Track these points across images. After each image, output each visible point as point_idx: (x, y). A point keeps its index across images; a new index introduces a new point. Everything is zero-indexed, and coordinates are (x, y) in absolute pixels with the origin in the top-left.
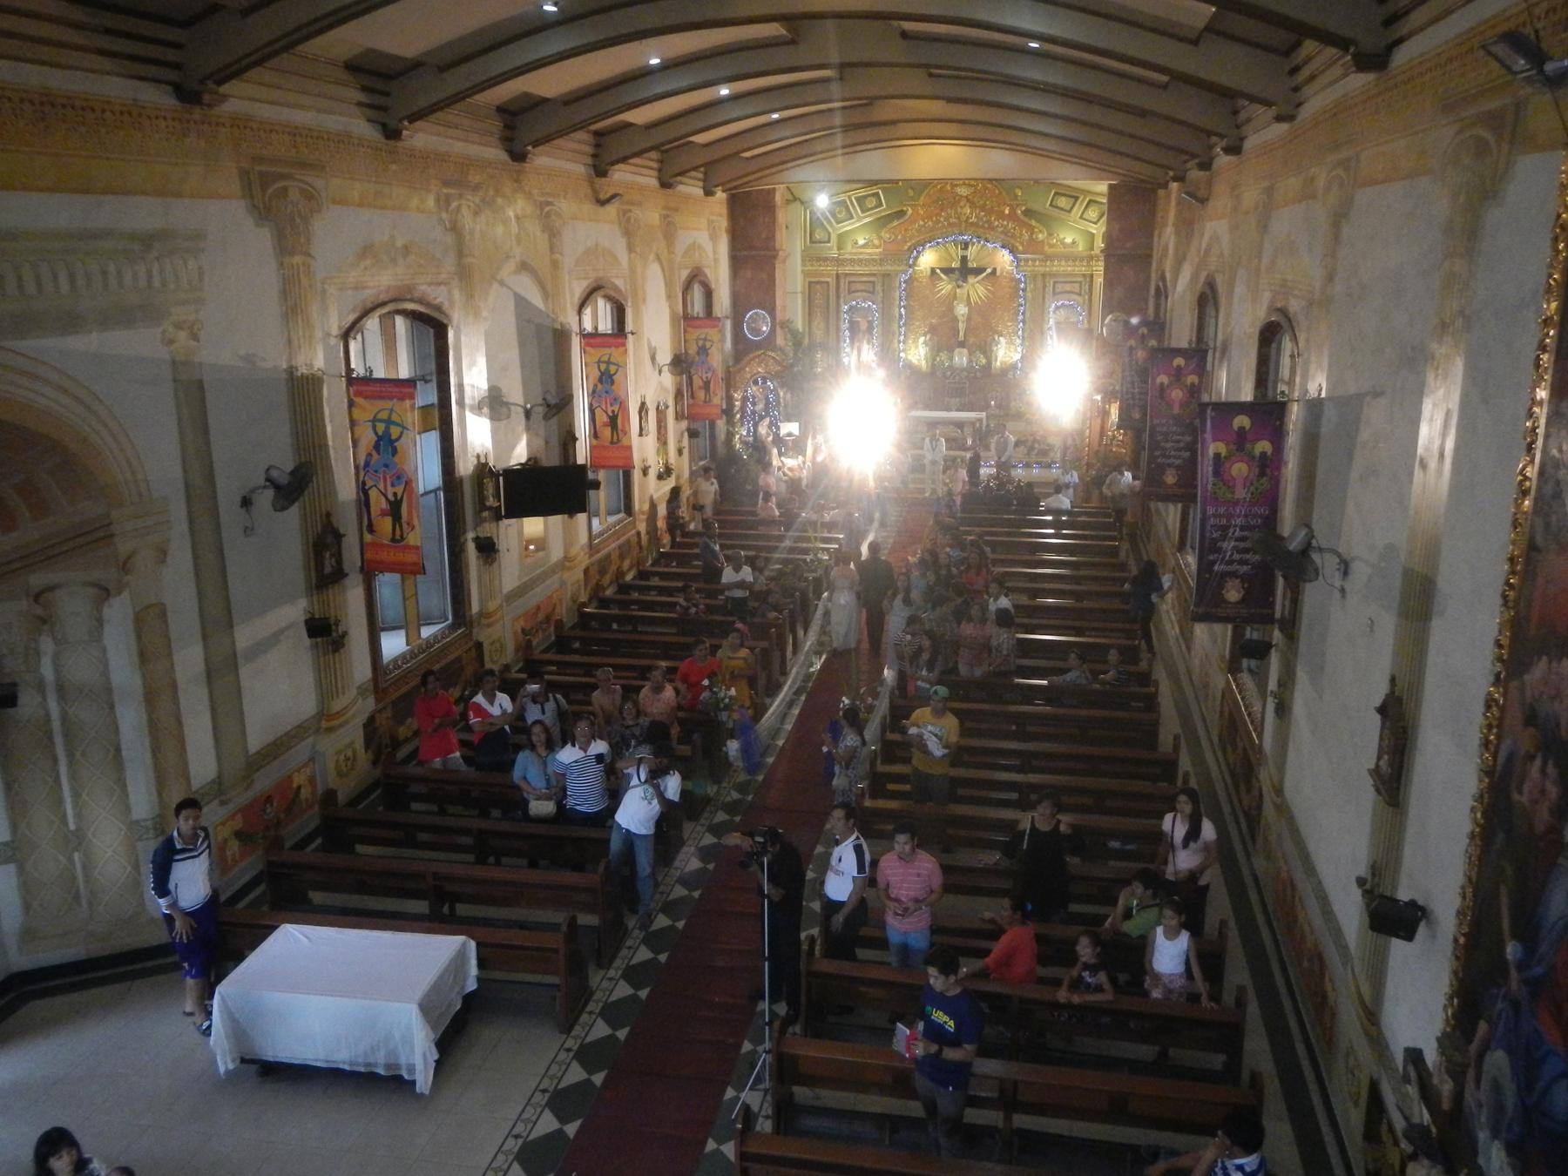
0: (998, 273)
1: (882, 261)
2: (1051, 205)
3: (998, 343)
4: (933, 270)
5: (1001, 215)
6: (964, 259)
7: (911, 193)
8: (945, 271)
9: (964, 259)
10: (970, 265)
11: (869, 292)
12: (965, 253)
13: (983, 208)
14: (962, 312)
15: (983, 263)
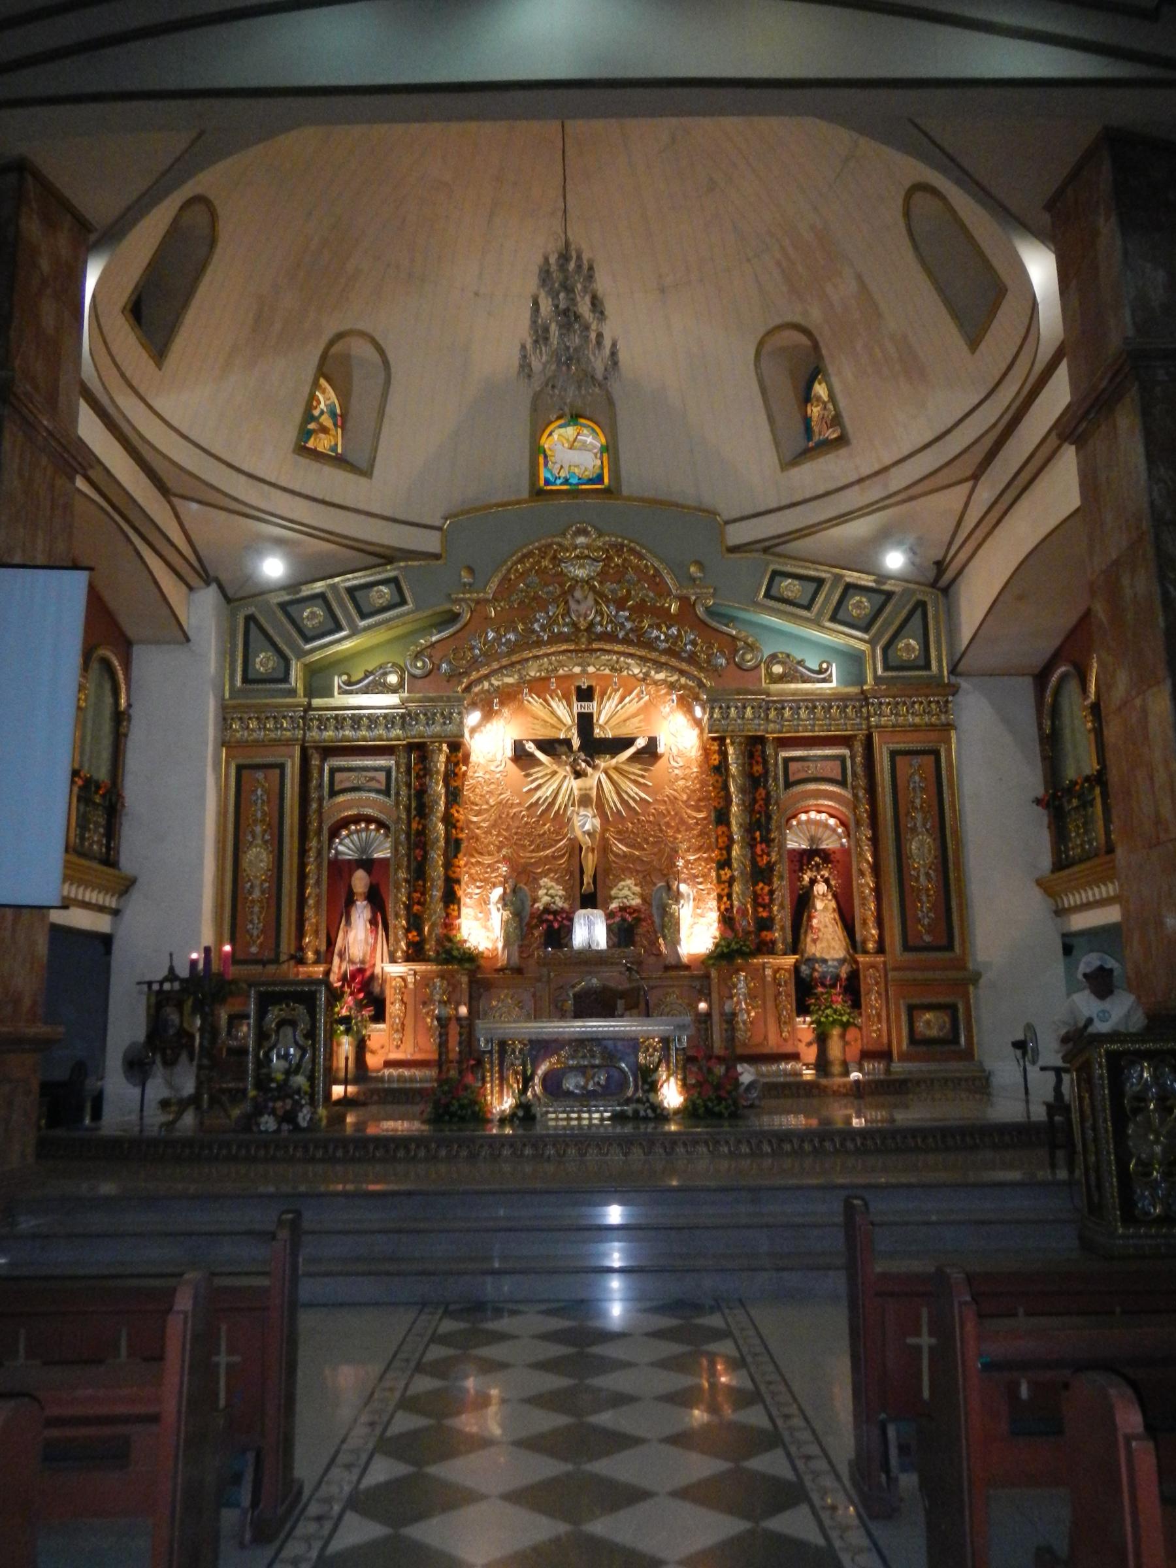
0: (661, 750)
1: (406, 719)
2: (767, 595)
3: (677, 897)
4: (518, 746)
5: (664, 617)
6: (585, 722)
7: (466, 578)
8: (548, 746)
9: (585, 722)
10: (598, 732)
11: (378, 791)
12: (592, 707)
13: (620, 604)
14: (588, 827)
15: (624, 732)
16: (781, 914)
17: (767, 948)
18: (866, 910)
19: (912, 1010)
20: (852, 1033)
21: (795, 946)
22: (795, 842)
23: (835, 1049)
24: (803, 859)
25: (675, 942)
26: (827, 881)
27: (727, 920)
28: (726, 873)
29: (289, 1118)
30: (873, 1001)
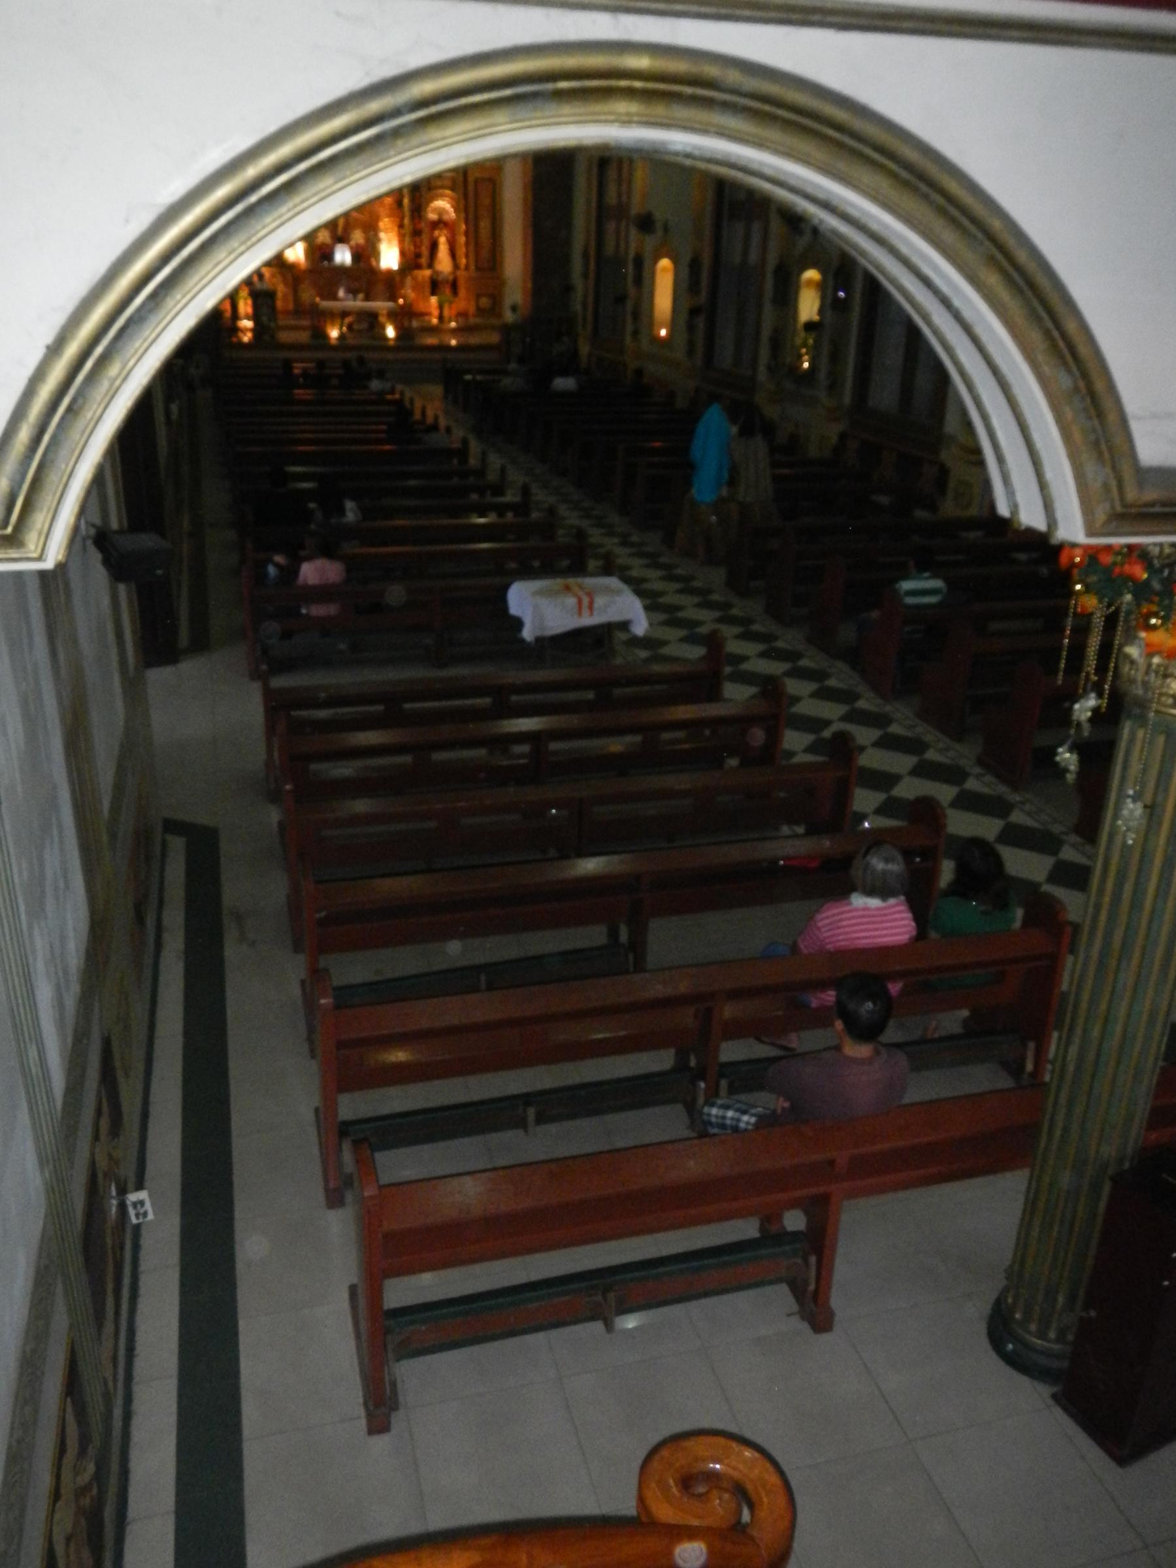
3: (379, 240)
16: (425, 251)
17: (419, 267)
18: (461, 251)
19: (478, 296)
20: (454, 306)
21: (430, 265)
22: (432, 216)
23: (446, 313)
24: (435, 225)
25: (378, 261)
26: (445, 235)
27: (403, 253)
28: (403, 231)
29: (273, 337)
30: (462, 292)
